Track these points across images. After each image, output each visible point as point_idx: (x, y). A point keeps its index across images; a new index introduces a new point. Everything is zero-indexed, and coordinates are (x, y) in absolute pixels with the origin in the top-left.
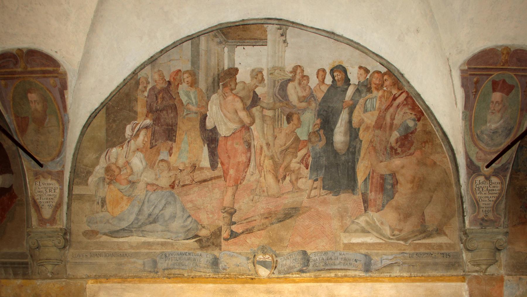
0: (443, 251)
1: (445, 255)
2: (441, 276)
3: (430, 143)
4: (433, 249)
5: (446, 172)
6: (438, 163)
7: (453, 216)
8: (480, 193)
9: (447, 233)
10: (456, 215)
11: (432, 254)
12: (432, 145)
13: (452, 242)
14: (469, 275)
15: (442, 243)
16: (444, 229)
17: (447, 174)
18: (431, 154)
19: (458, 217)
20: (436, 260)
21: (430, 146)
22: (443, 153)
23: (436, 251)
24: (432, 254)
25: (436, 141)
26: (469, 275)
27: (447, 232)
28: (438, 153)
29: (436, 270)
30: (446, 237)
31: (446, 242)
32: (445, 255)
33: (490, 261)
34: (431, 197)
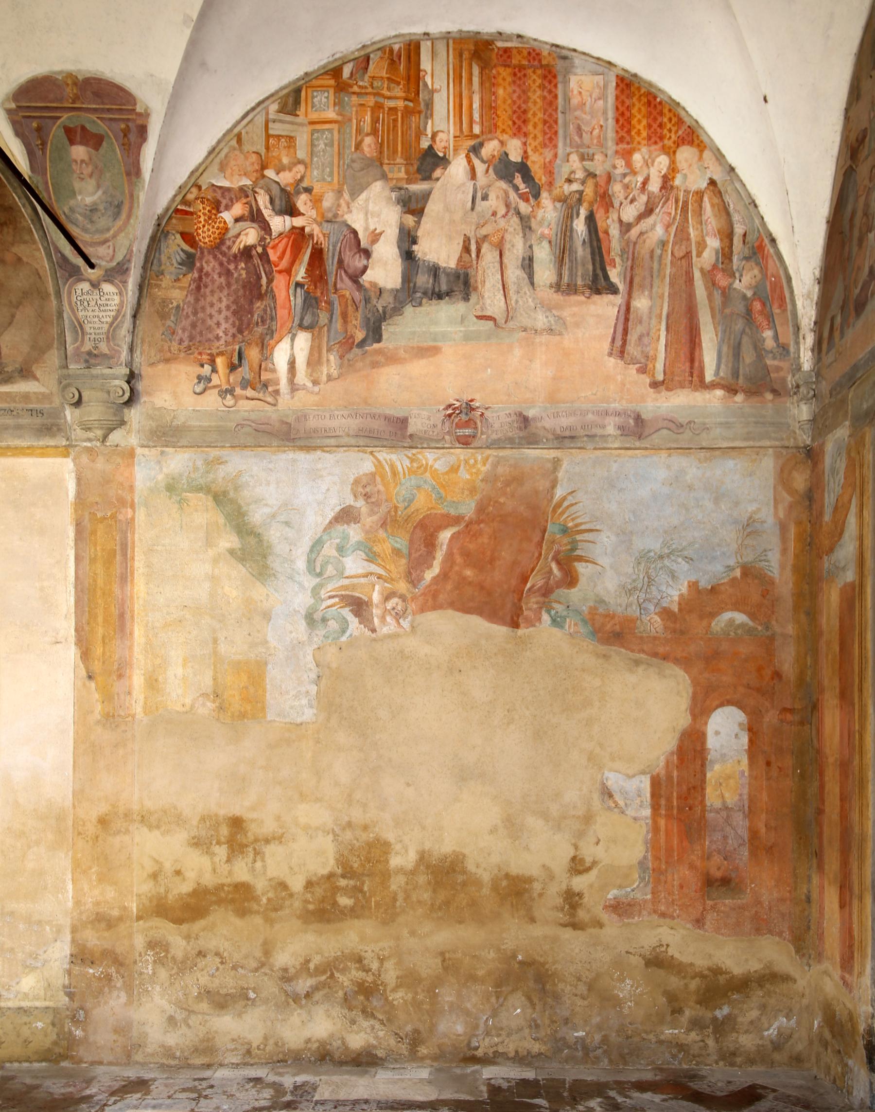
0: (31, 406)
1: (34, 413)
2: (28, 448)
3: (11, 226)
4: (15, 402)
5: (38, 274)
6: (25, 259)
7: (49, 347)
8: (85, 309)
9: (38, 376)
10: (55, 346)
11: (12, 411)
12: (15, 229)
13: (47, 391)
14: (76, 446)
15: (29, 393)
16: (33, 368)
17: (40, 278)
18: (13, 244)
19: (58, 349)
20: (20, 420)
21: (11, 231)
22: (34, 242)
23: (20, 406)
24: (12, 411)
25: (21, 222)
26: (76, 446)
27: (38, 374)
28: (25, 242)
29: (20, 437)
30: (36, 383)
31: (36, 390)
32: (34, 413)
33: (105, 422)
34: (13, 316)
